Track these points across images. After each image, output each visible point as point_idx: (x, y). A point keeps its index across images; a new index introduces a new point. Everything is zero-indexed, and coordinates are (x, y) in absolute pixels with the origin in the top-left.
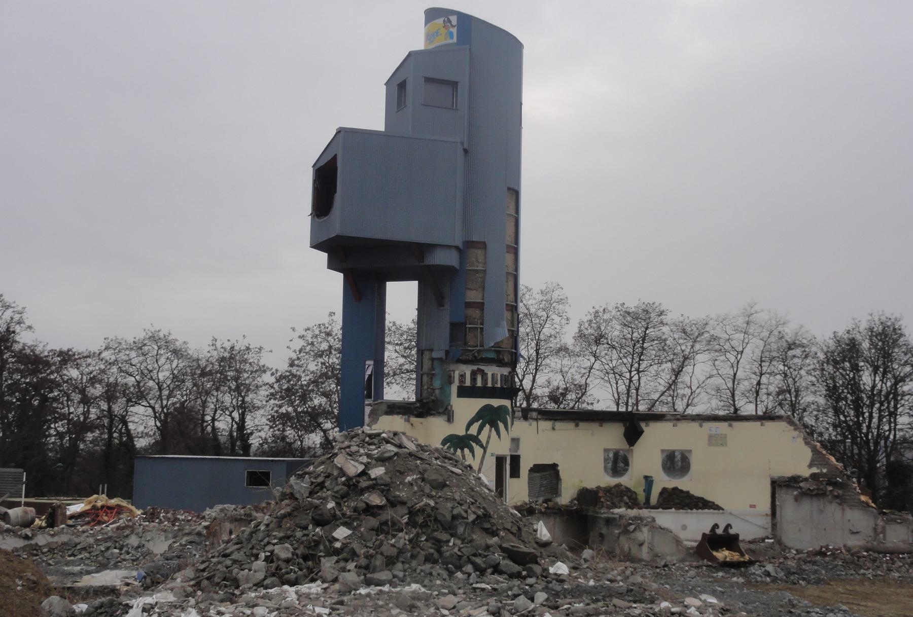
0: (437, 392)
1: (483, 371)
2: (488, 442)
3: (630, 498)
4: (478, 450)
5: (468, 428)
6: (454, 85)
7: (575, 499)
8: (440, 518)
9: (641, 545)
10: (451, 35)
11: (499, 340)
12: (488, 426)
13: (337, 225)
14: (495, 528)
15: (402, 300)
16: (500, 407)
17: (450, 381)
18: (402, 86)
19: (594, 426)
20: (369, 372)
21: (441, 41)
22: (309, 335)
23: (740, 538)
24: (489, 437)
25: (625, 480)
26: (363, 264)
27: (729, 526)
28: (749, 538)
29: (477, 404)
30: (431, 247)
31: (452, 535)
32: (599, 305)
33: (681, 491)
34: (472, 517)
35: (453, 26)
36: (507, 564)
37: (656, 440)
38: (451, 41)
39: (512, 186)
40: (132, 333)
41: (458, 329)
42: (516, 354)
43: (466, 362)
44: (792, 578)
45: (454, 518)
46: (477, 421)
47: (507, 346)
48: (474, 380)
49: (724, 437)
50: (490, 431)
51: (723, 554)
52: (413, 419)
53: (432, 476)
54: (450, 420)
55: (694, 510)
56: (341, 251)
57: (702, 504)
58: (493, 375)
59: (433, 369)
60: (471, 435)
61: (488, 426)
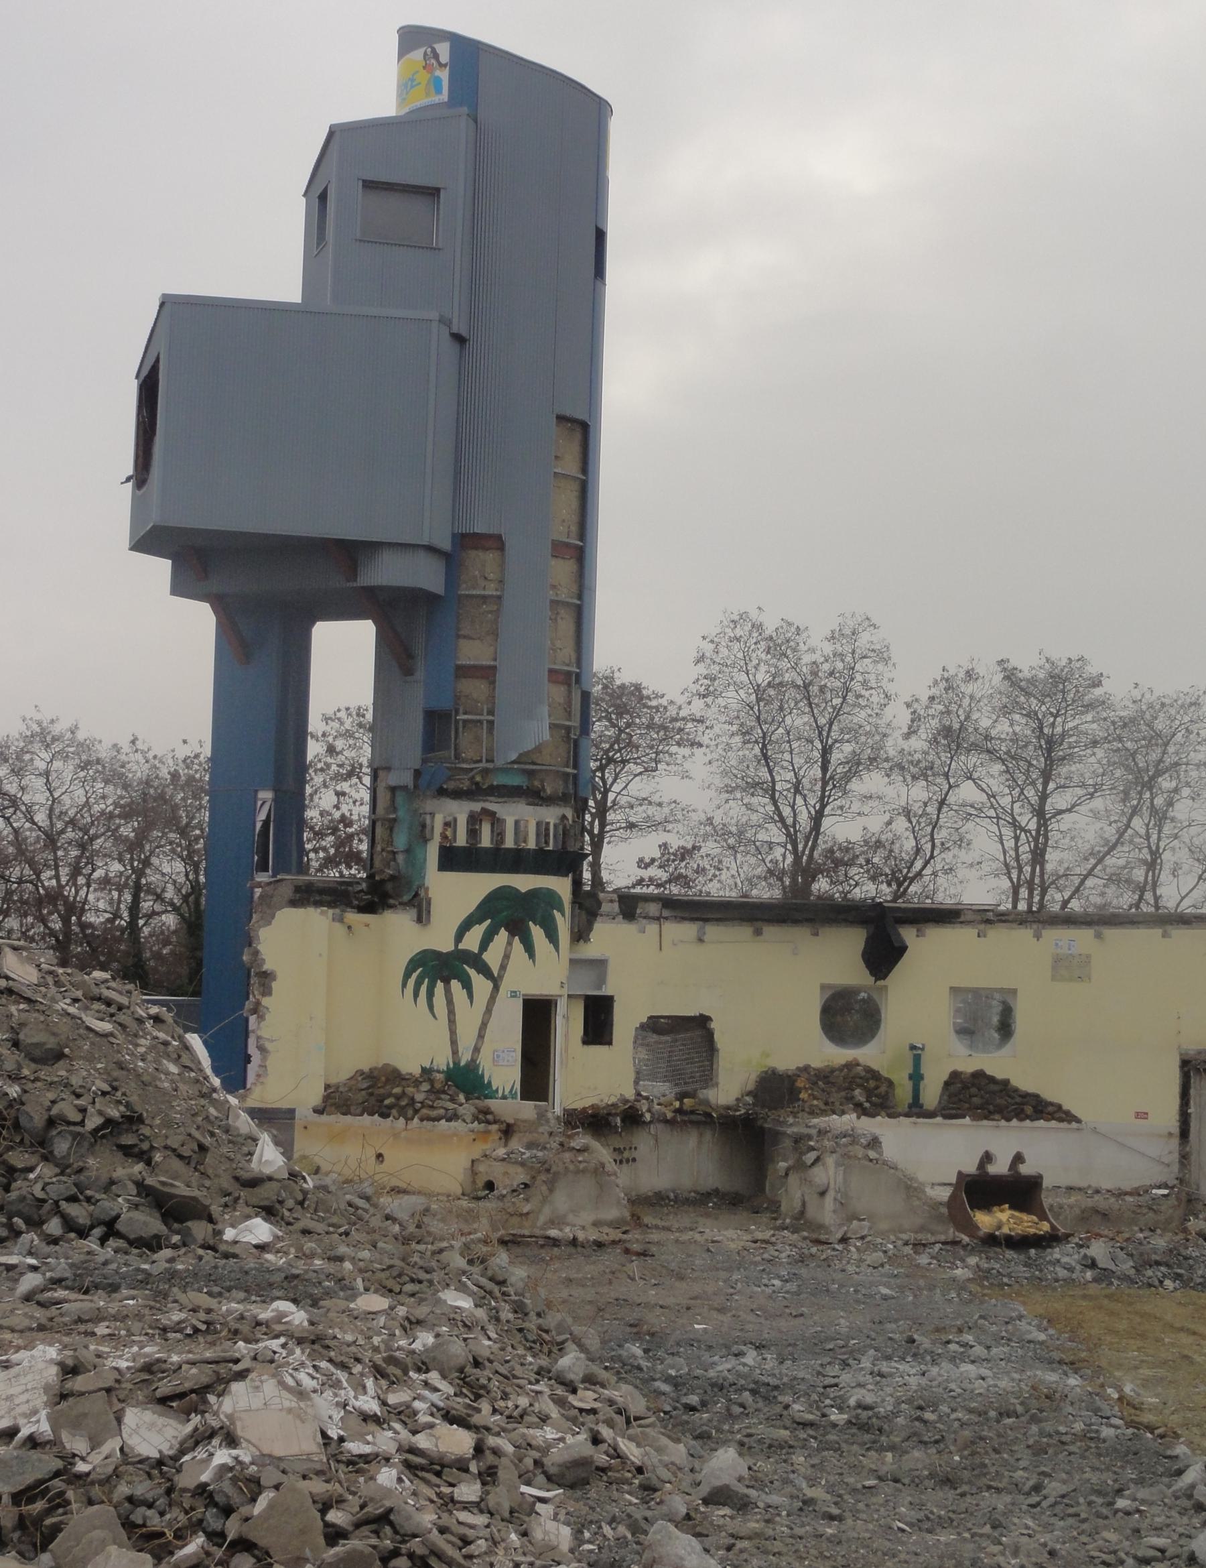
0: (400, 858)
1: (492, 814)
2: (503, 967)
3: (869, 1093)
5: (459, 937)
6: (433, 193)
7: (749, 1094)
8: (23, 1121)
9: (823, 1194)
10: (437, 83)
11: (529, 745)
12: (503, 934)
14: (145, 1146)
15: (343, 660)
16: (534, 894)
17: (422, 834)
18: (323, 197)
19: (800, 934)
20: (262, 816)
21: (421, 99)
23: (1047, 1183)
24: (507, 956)
25: (868, 1055)
26: (257, 585)
27: (1018, 1158)
28: (1064, 1181)
29: (478, 886)
30: (373, 547)
31: (45, 1158)
32: (956, 664)
33: (992, 1080)
34: (93, 1122)
35: (441, 65)
36: (149, 1222)
37: (934, 969)
38: (436, 99)
39: (568, 412)
41: (438, 725)
42: (575, 777)
43: (457, 794)
44: (1149, 1273)
45: (51, 1122)
46: (480, 922)
47: (553, 758)
48: (473, 833)
49: (1086, 960)
50: (510, 943)
51: (1001, 1219)
52: (352, 917)
53: (29, 1036)
54: (423, 916)
55: (1015, 1122)
56: (196, 555)
57: (1036, 1108)
58: (517, 823)
59: (395, 810)
61: (503, 934)
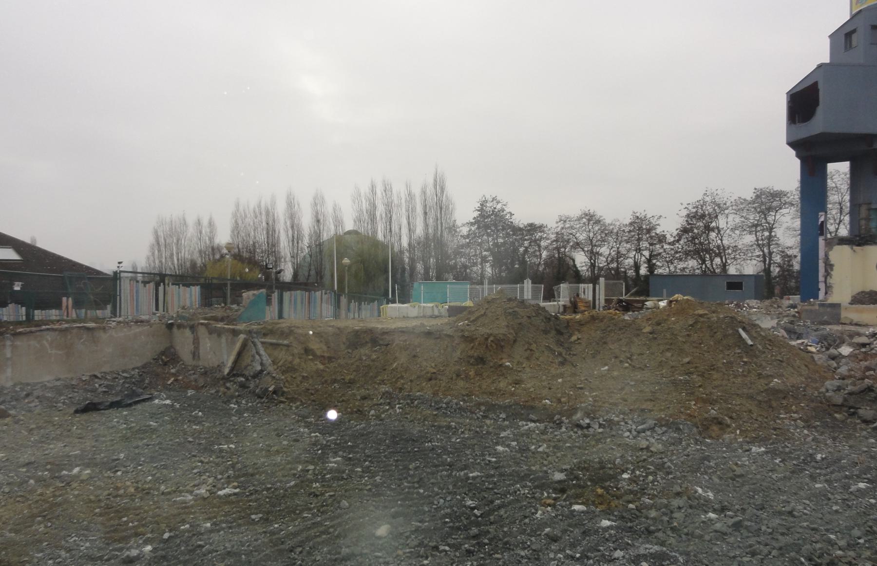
13: (818, 124)
22: (690, 207)
40: (574, 210)
52: (855, 248)
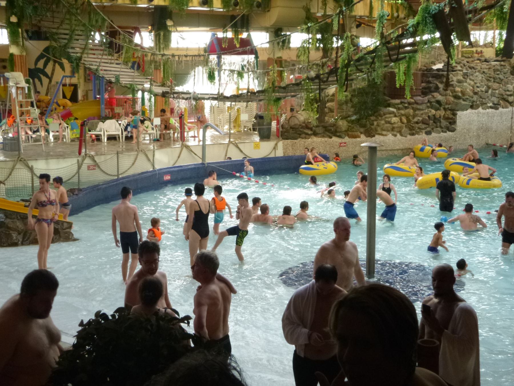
2: (52, 74)
4: (45, 80)
5: (36, 63)
24: (53, 70)
50: (54, 65)
60: (39, 69)
